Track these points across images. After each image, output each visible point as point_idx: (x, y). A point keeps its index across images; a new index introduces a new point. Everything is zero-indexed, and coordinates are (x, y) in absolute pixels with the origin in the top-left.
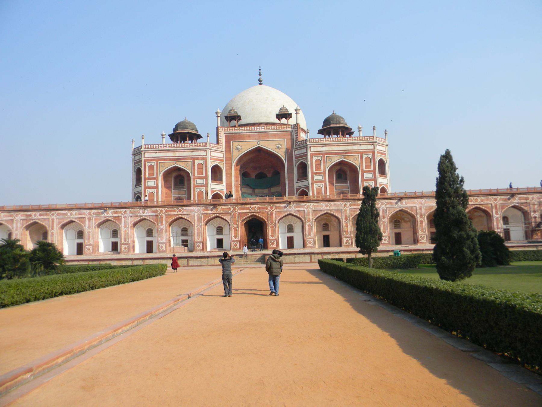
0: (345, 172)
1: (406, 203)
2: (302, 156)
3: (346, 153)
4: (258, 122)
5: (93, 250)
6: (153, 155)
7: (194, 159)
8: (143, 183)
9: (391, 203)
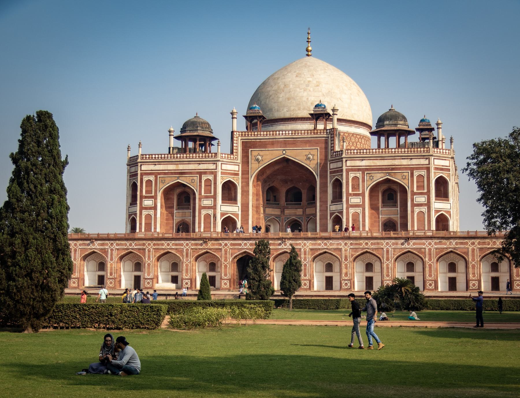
0: (396, 192)
1: (414, 244)
2: (338, 171)
3: (393, 169)
4: (294, 116)
5: (78, 283)
6: (152, 167)
7: (201, 174)
8: (138, 202)
9: (397, 244)
